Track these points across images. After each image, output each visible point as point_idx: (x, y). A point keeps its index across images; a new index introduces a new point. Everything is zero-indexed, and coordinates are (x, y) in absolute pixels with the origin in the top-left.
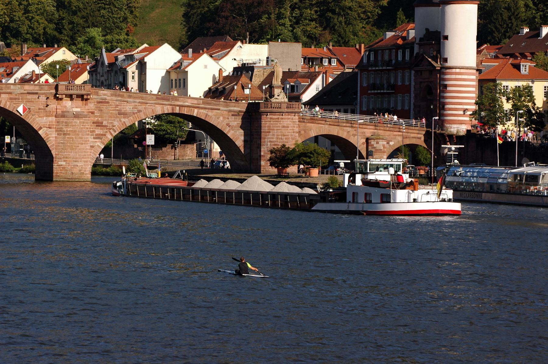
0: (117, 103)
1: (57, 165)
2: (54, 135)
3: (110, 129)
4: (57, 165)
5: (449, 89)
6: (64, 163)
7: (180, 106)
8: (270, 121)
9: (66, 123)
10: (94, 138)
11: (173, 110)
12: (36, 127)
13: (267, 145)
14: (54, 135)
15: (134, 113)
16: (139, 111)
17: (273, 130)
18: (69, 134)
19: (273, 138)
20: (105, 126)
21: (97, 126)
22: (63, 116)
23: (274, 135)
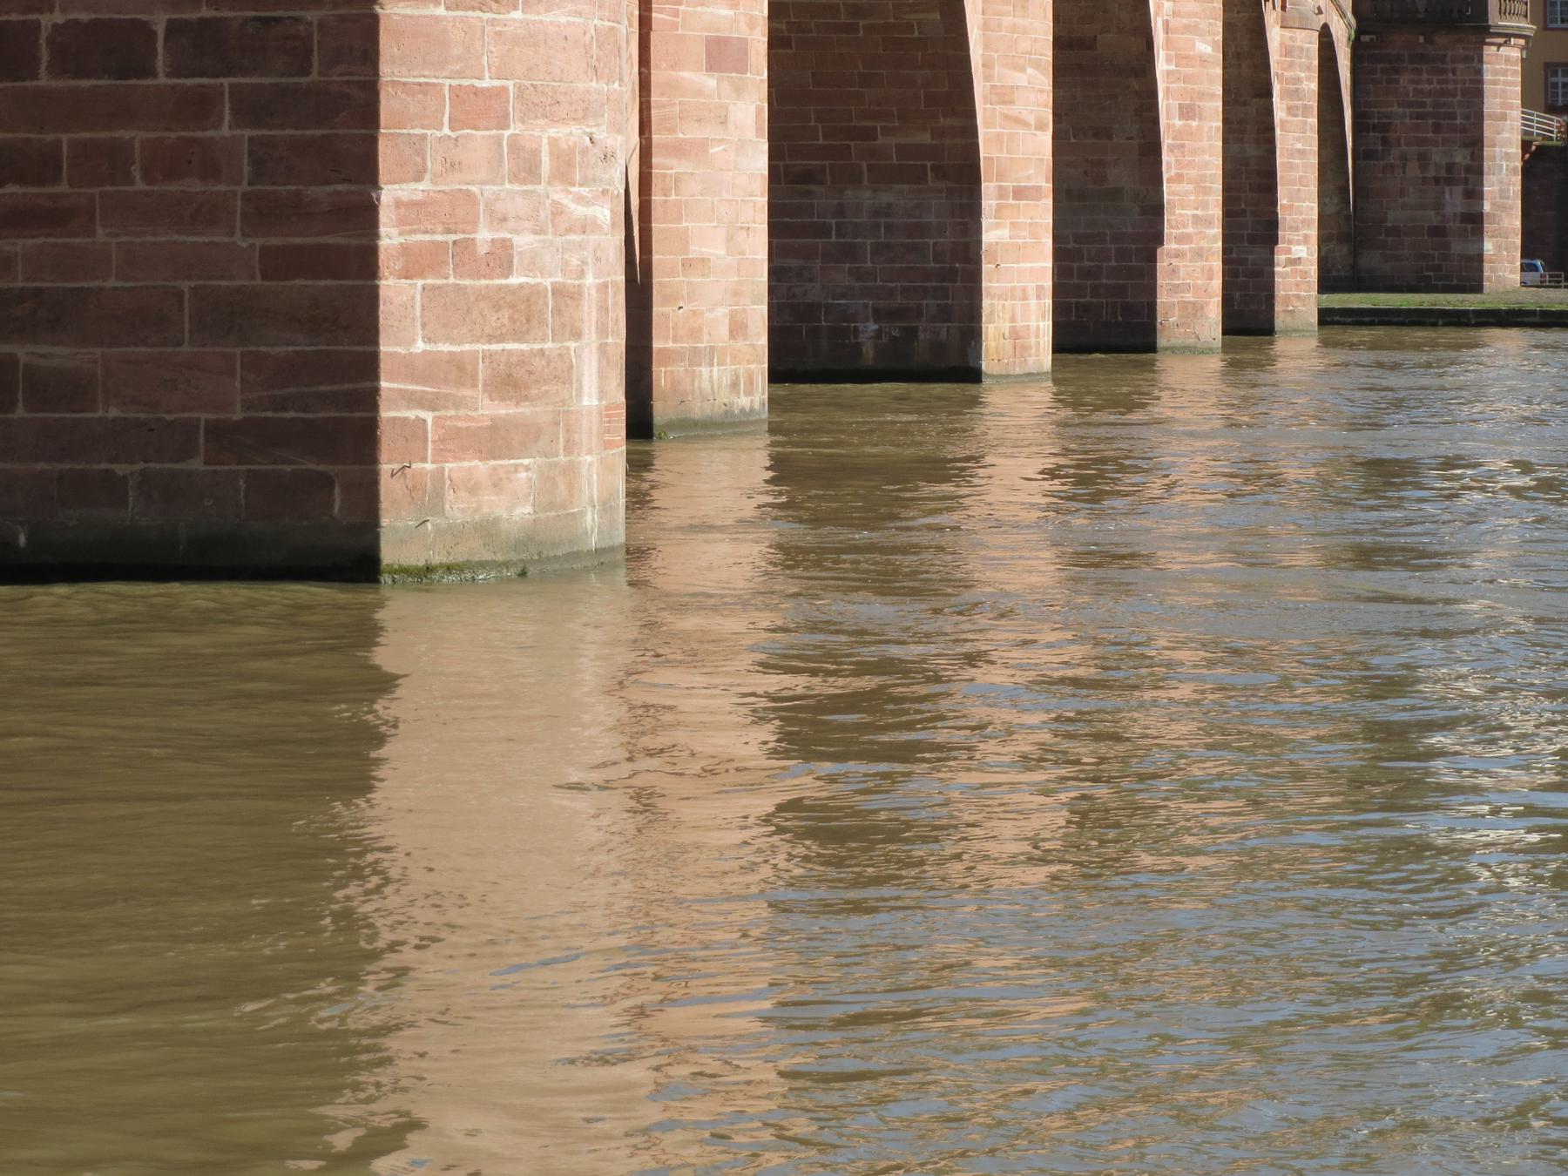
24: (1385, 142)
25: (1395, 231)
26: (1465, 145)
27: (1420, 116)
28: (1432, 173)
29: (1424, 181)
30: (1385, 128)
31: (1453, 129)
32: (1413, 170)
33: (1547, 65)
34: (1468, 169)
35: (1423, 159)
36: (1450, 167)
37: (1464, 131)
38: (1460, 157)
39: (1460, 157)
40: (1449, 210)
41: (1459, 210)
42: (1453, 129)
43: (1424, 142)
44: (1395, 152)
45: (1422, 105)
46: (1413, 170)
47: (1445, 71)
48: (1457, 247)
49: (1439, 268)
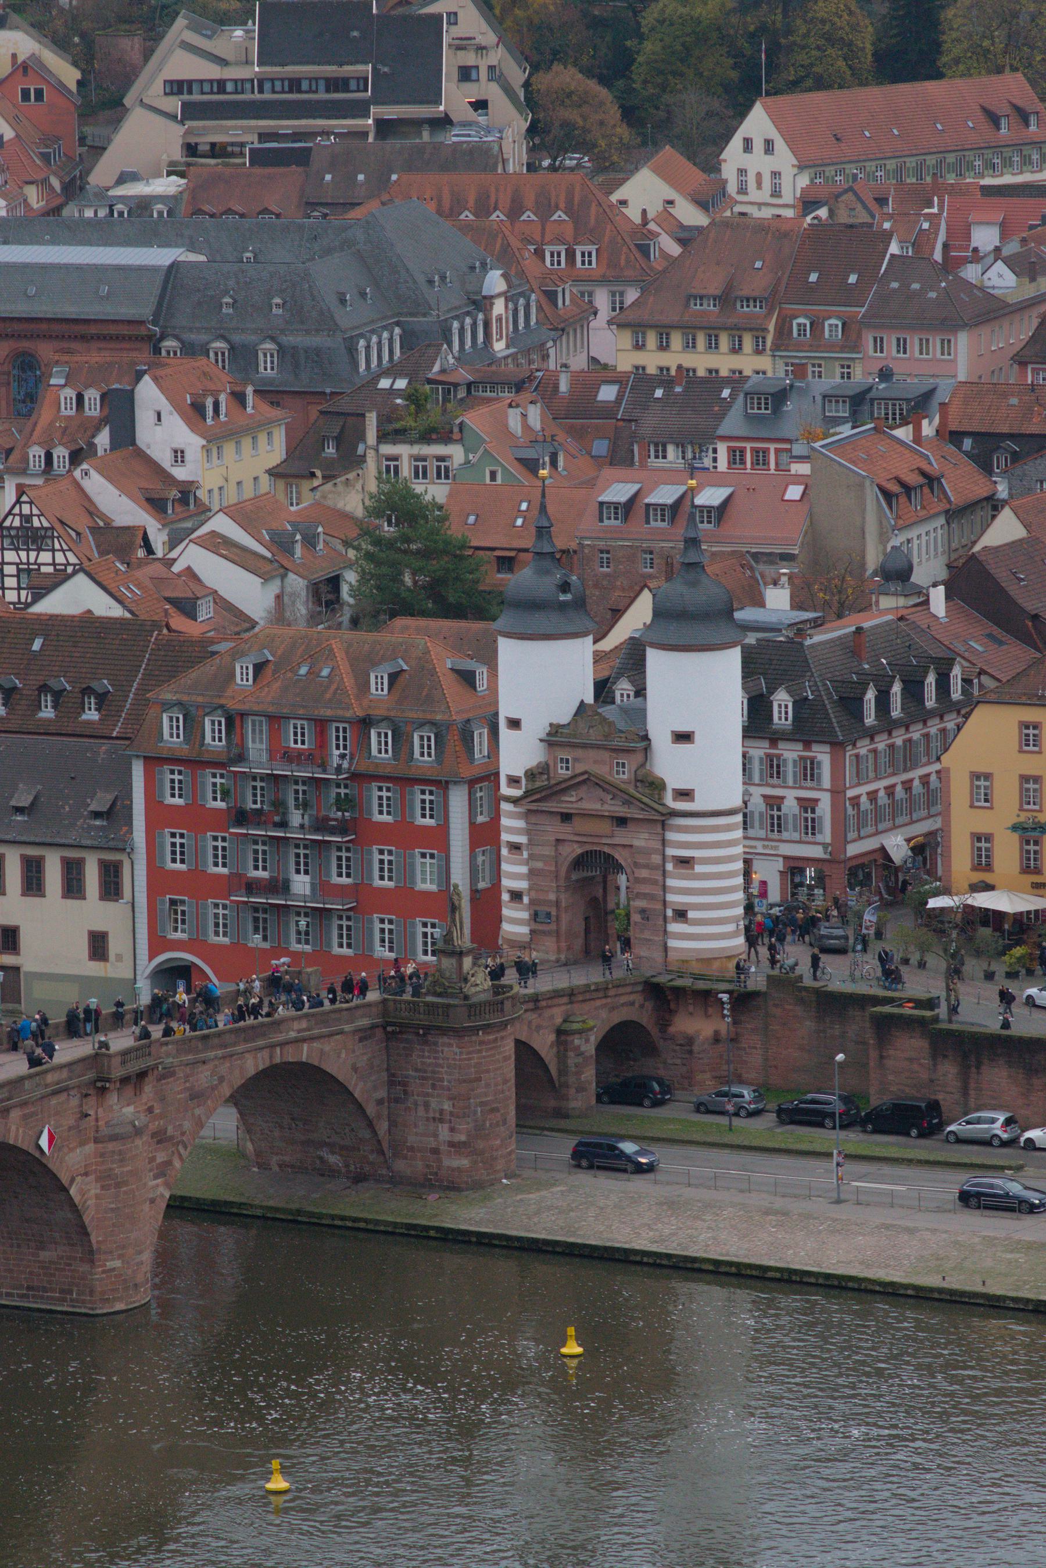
0: (188, 1070)
1: (104, 1272)
2: (94, 1190)
3: (178, 1143)
4: (104, 1272)
5: (699, 869)
6: (117, 1263)
7: (283, 1044)
8: (480, 1051)
9: (120, 1152)
10: (156, 1177)
11: (271, 1057)
12: (65, 1181)
13: (475, 1113)
14: (93, 1192)
15: (213, 1088)
16: (221, 1079)
17: (488, 1071)
18: (126, 1183)
19: (486, 1095)
20: (172, 1138)
21: (159, 1142)
22: (114, 1138)
23: (488, 1085)
24: (405, 1092)
25: (412, 1149)
26: (450, 1099)
27: (424, 1078)
28: (431, 1115)
29: (428, 1119)
30: (405, 1084)
31: (442, 1088)
32: (421, 1112)
33: (973, 834)
34: (451, 1114)
35: (426, 1105)
36: (441, 1111)
37: (449, 1089)
38: (447, 1106)
39: (447, 1106)
40: (441, 1138)
41: (448, 1139)
42: (442, 1088)
43: (428, 1095)
44: (411, 1099)
45: (425, 1071)
46: (421, 1112)
47: (437, 1052)
48: (447, 1162)
49: (436, 1174)
